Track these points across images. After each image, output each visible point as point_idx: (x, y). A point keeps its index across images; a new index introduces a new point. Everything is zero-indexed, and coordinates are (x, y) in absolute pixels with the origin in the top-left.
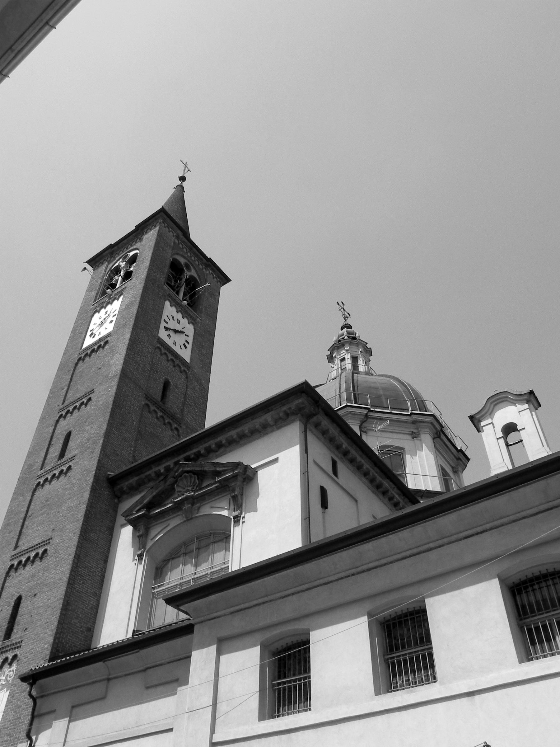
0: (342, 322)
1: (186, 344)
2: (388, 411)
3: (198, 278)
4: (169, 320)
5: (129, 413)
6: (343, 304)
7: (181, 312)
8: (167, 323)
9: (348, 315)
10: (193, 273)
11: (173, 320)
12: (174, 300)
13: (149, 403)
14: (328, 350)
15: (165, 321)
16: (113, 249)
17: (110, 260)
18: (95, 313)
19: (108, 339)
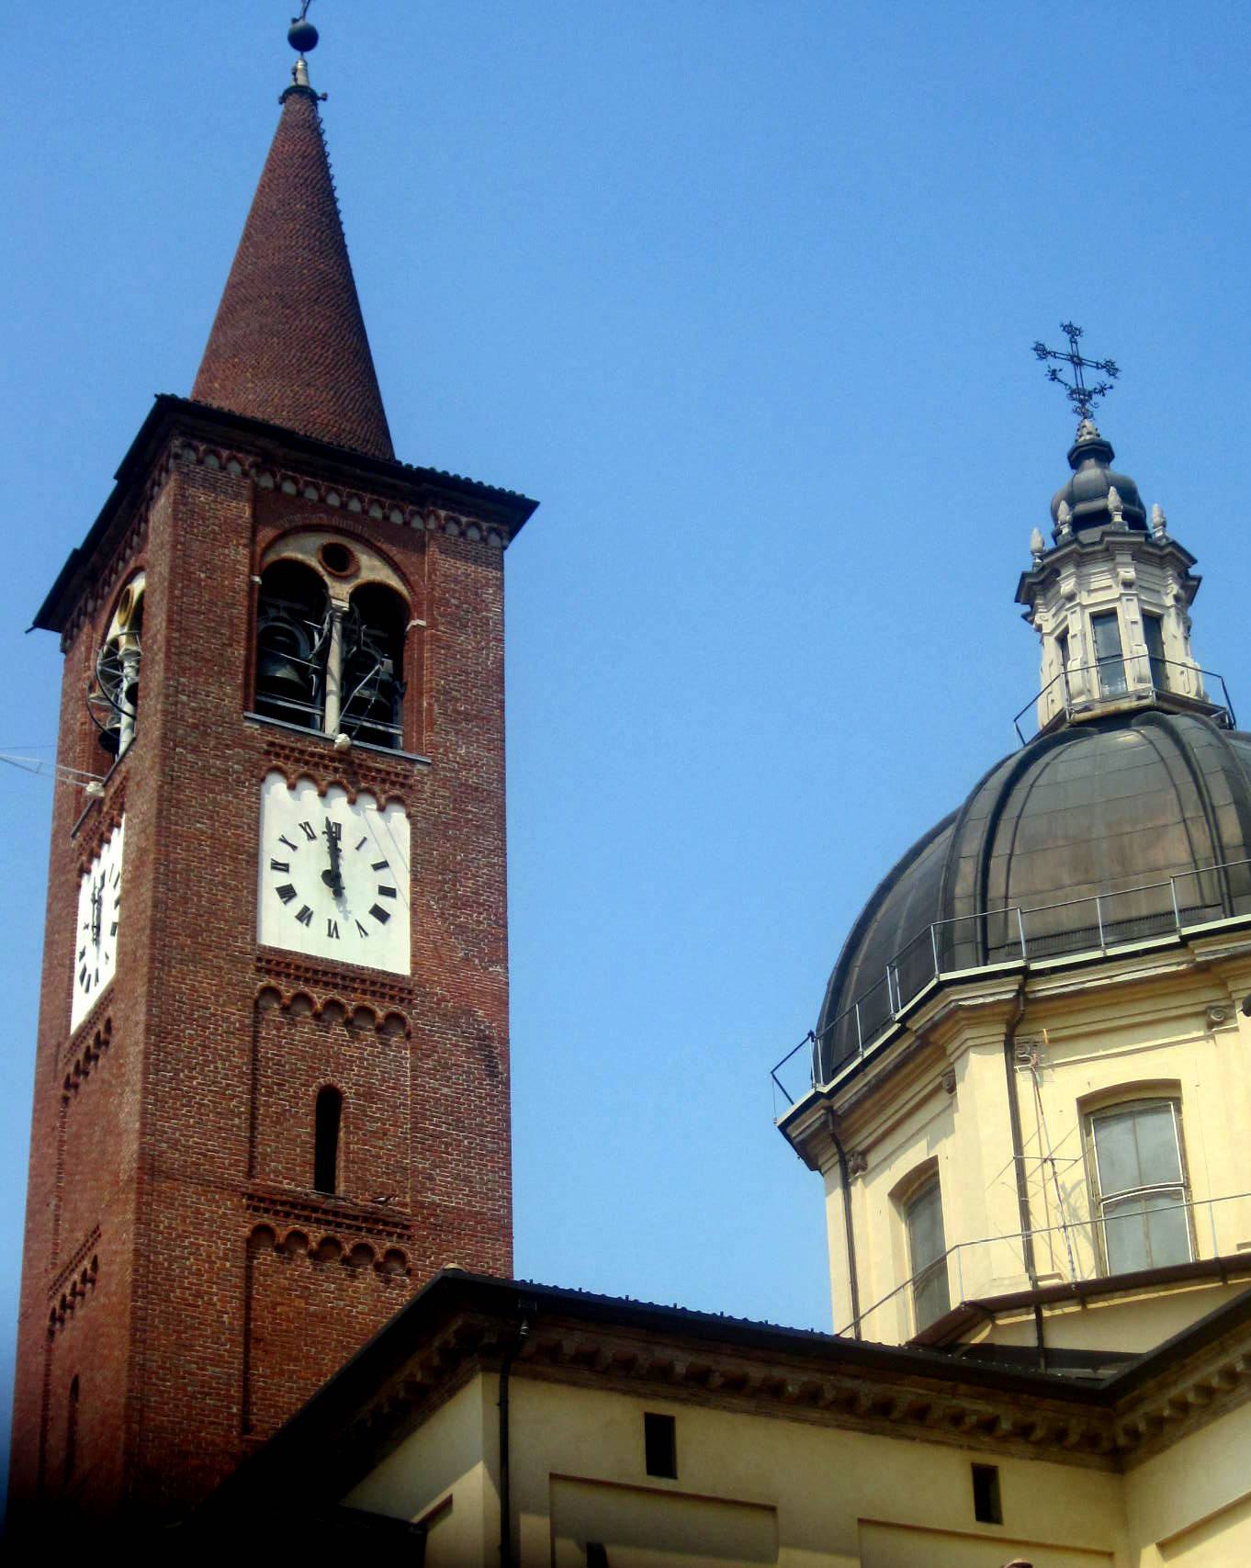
0: (1066, 431)
1: (385, 903)
2: (1097, 954)
3: (395, 582)
4: (294, 848)
5: (199, 1295)
6: (1072, 331)
7: (336, 784)
8: (284, 868)
9: (1102, 376)
10: (372, 569)
11: (312, 837)
12: (300, 757)
13: (267, 1219)
14: (1017, 601)
15: (276, 866)
16: (89, 566)
17: (95, 609)
18: (80, 876)
19: (110, 1012)
